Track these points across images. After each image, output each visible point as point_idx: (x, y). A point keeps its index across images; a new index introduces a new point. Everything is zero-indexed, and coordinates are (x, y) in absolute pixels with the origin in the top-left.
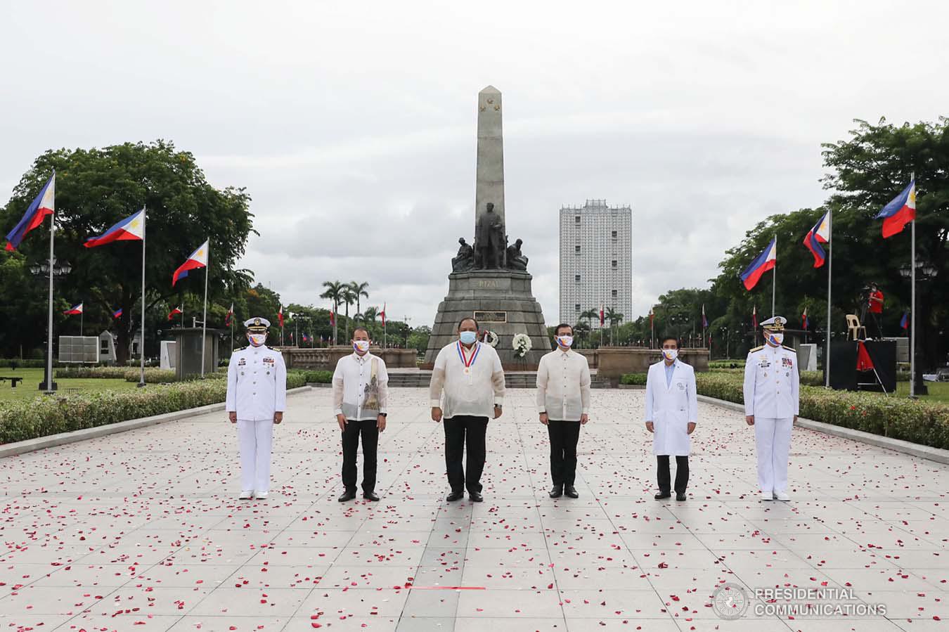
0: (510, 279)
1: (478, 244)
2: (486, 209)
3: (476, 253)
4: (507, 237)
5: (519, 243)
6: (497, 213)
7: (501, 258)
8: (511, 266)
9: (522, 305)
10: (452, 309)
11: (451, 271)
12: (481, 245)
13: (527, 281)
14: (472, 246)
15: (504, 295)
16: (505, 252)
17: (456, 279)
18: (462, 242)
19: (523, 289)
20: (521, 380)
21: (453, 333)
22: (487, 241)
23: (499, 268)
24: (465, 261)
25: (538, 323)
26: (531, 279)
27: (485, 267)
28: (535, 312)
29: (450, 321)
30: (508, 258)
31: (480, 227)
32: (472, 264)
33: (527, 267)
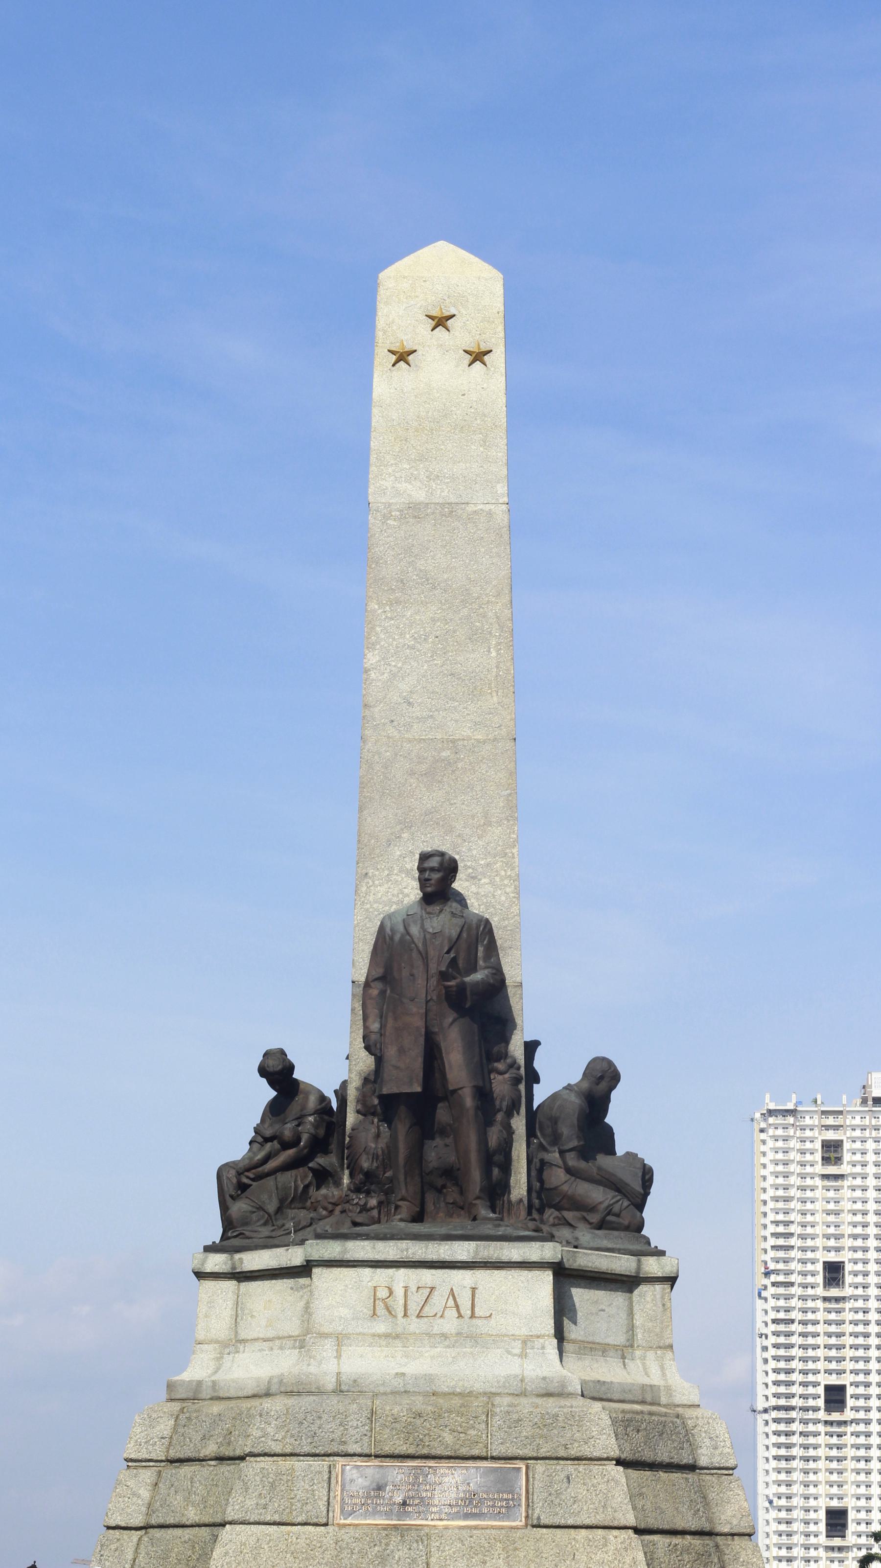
0: (548, 1277)
1: (372, 1080)
2: (412, 892)
4: (531, 1047)
7: (498, 1160)
8: (548, 1209)
9: (624, 1425)
10: (211, 1449)
11: (215, 1233)
13: (647, 1294)
16: (519, 1124)
18: (278, 1072)
19: (619, 1339)
22: (415, 1061)
23: (484, 1212)
24: (288, 1179)
25: (710, 1534)
26: (671, 1280)
29: (192, 1515)
30: (538, 1170)
32: (327, 1192)
33: (647, 1213)
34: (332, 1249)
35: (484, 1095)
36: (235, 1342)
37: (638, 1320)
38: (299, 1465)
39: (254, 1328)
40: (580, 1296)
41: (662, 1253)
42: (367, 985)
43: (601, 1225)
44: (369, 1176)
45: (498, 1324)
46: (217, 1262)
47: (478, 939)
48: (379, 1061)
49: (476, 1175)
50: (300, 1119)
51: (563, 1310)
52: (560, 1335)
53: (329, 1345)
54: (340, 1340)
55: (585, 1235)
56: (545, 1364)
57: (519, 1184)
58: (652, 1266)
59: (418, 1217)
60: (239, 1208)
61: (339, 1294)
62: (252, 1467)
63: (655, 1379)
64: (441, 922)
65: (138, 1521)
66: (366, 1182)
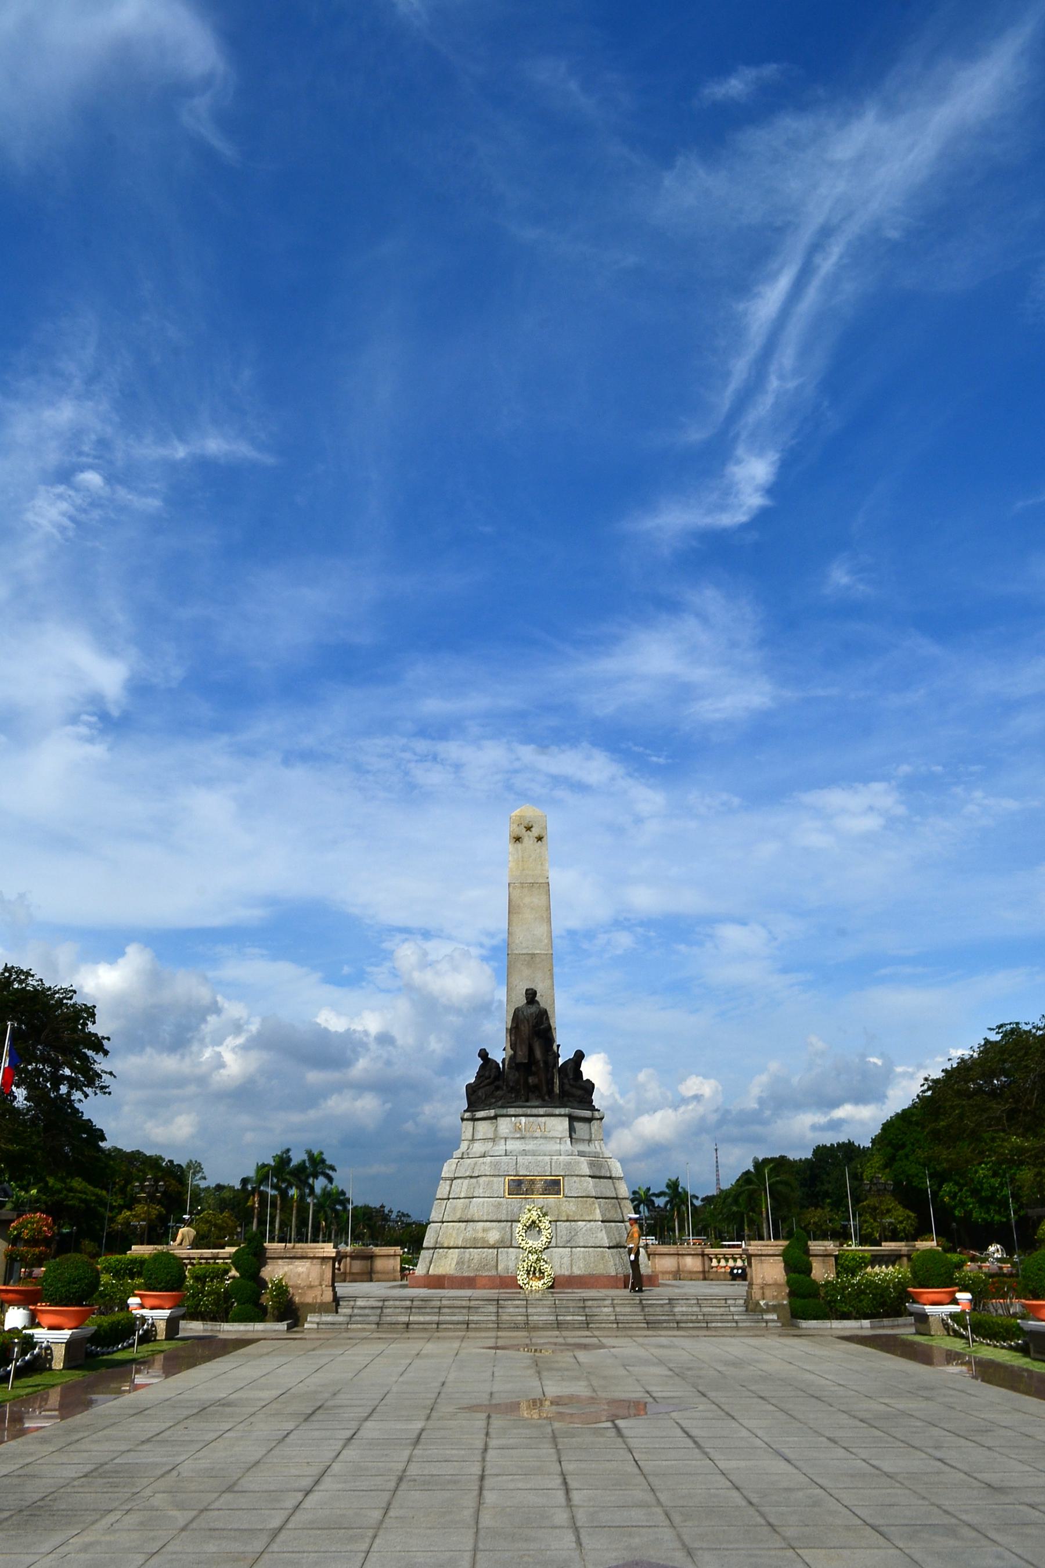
1: (513, 1058)
3: (513, 1076)
4: (558, 1046)
5: (579, 1056)
6: (543, 1005)
7: (551, 1083)
9: (591, 1165)
12: (518, 1061)
14: (500, 1062)
15: (557, 1147)
17: (474, 1119)
18: (483, 1054)
19: (587, 1137)
20: (606, 1310)
21: (469, 1217)
25: (617, 1198)
26: (601, 1119)
27: (523, 1099)
28: (610, 1178)
29: (462, 1195)
30: (562, 1085)
31: (515, 1030)
32: (499, 1093)
34: (504, 1111)
35: (546, 1063)
36: (473, 1140)
37: (593, 1131)
38: (495, 1179)
39: (478, 1136)
40: (578, 1125)
41: (598, 1110)
42: (511, 1029)
43: (580, 1102)
44: (512, 1088)
45: (552, 1134)
46: (467, 1115)
47: (543, 1016)
48: (515, 1052)
49: (545, 1089)
50: (490, 1070)
51: (572, 1130)
52: (571, 1137)
53: (503, 1141)
54: (506, 1139)
55: (576, 1104)
56: (567, 1145)
57: (557, 1090)
58: (597, 1115)
59: (527, 1101)
60: (473, 1098)
61: (505, 1125)
62: (482, 1180)
63: (598, 1149)
64: (533, 1009)
65: (446, 1197)
66: (512, 1090)
